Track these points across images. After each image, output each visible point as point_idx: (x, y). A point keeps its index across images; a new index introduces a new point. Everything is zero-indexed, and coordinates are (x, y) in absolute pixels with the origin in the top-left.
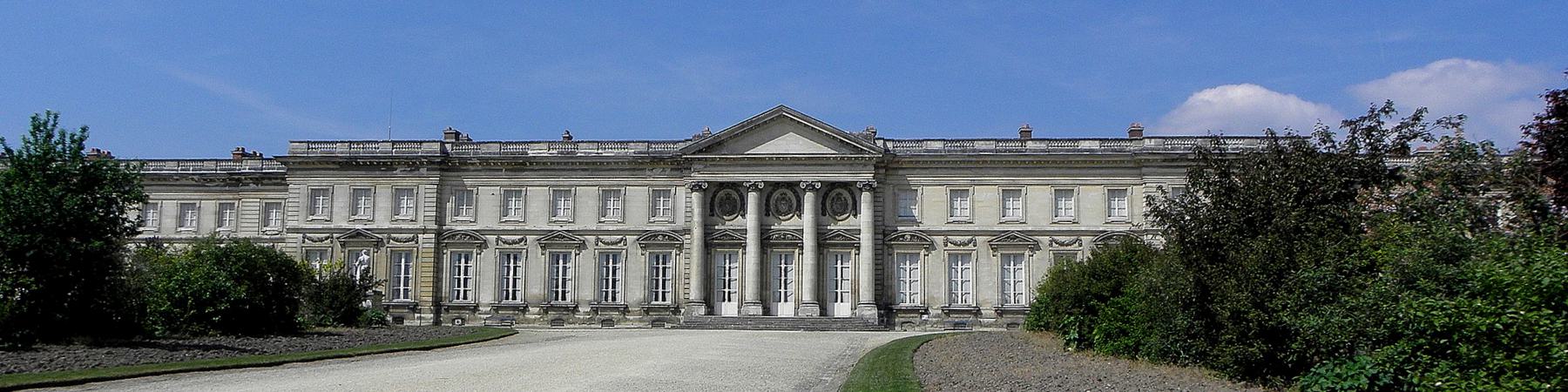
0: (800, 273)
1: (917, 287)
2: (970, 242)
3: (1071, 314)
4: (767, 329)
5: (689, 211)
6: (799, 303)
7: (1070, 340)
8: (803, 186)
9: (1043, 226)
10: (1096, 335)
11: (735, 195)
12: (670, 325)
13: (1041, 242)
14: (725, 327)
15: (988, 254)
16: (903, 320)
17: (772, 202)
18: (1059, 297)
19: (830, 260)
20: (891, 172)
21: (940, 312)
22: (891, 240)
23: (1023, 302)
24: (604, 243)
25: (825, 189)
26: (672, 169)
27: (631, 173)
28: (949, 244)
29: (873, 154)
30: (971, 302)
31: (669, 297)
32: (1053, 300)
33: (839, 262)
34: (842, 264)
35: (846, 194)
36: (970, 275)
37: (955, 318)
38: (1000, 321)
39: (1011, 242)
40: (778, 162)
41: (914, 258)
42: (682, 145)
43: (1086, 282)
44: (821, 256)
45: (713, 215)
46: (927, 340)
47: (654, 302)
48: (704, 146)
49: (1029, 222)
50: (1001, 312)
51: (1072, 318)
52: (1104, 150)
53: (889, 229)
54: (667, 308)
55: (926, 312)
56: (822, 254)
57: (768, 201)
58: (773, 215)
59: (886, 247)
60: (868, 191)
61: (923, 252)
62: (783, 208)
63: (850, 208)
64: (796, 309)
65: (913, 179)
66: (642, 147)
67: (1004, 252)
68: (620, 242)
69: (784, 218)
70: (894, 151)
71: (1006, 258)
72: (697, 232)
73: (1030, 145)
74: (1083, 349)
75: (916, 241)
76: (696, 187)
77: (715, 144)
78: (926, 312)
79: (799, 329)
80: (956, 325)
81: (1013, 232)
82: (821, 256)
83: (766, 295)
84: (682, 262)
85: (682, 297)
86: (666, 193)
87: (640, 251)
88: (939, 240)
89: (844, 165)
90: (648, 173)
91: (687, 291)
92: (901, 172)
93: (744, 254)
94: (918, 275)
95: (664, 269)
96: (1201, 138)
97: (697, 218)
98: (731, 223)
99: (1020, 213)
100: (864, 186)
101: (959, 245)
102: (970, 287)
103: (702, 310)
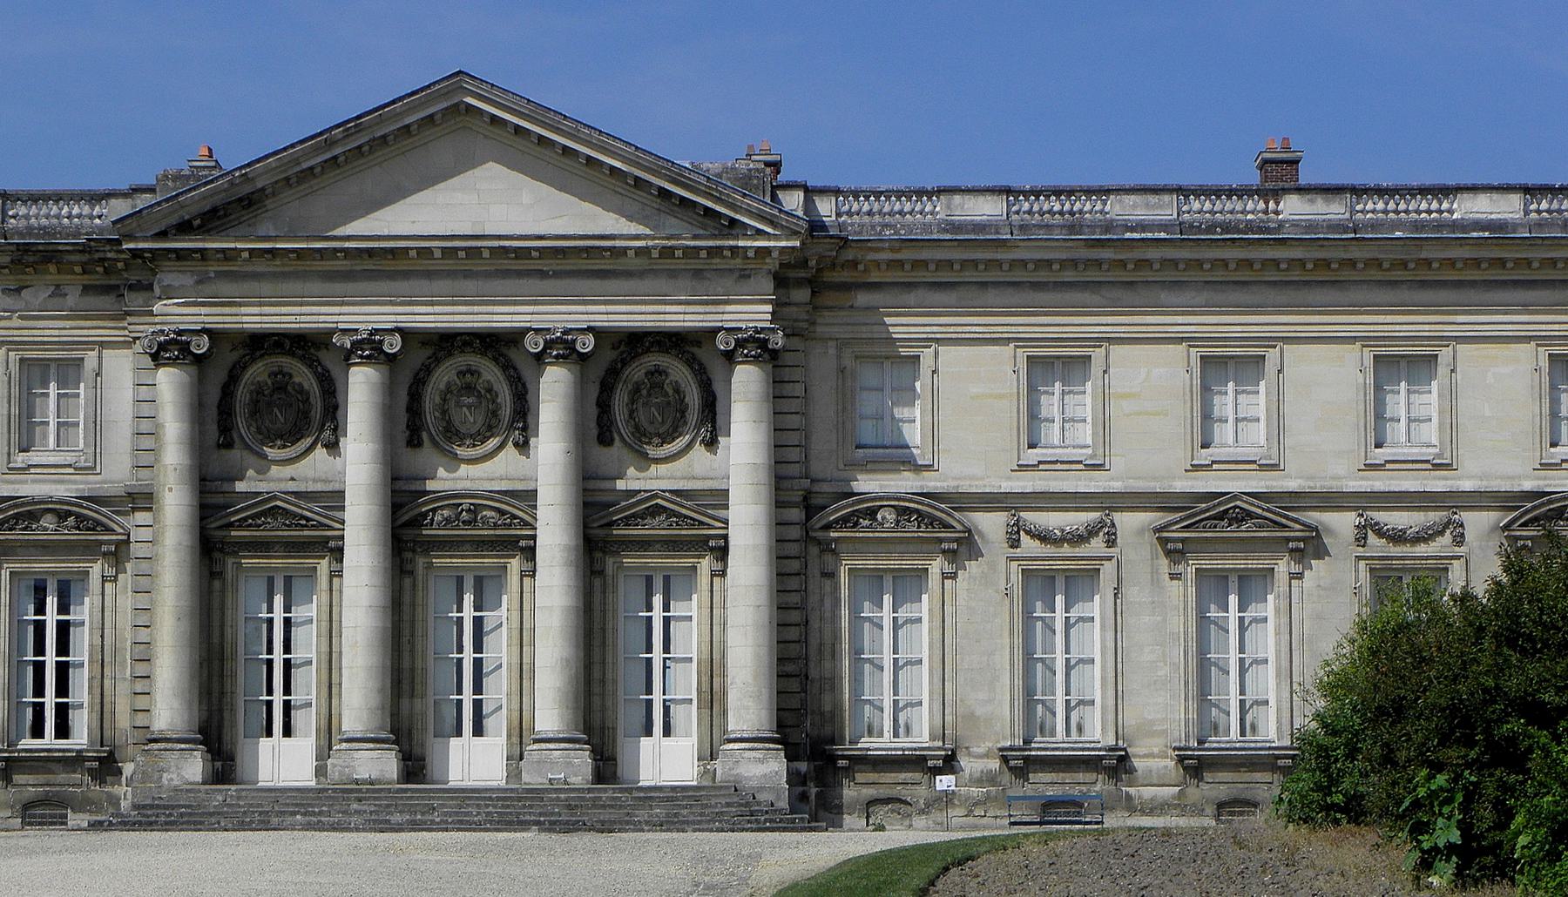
0: (524, 638)
1: (921, 684)
2: (1092, 532)
3: (1437, 767)
4: (415, 826)
5: (146, 433)
6: (521, 735)
7: (1435, 849)
8: (533, 344)
9: (1339, 478)
10: (1518, 834)
11: (303, 376)
12: (82, 819)
13: (1329, 531)
14: (275, 820)
15: (1154, 572)
16: (869, 792)
17: (431, 399)
18: (1397, 711)
19: (627, 593)
20: (829, 298)
21: (995, 764)
22: (828, 527)
23: (1272, 731)
25: (609, 355)
26: (86, 289)
28: (1024, 538)
29: (776, 237)
30: (1097, 734)
31: (81, 723)
32: (1375, 722)
33: (657, 600)
34: (666, 608)
35: (679, 373)
36: (1093, 641)
37: (1046, 784)
38: (1194, 793)
39: (1231, 532)
40: (449, 264)
41: (909, 583)
42: (120, 208)
43: (1486, 660)
44: (597, 582)
45: (228, 445)
46: (959, 857)
47: (28, 743)
48: (195, 209)
49: (1291, 463)
50: (1195, 766)
51: (1441, 780)
52: (1540, 225)
53: (825, 488)
54: (75, 761)
55: (949, 763)
56: (601, 573)
57: (415, 396)
58: (435, 444)
59: (814, 550)
60: (756, 360)
61: (936, 566)
62: (468, 416)
63: (693, 416)
64: (516, 758)
65: (901, 326)
67: (1206, 564)
70: (841, 227)
71: (1213, 585)
73: (1292, 207)
74: (1476, 882)
75: (912, 529)
76: (166, 351)
78: (949, 763)
79: (523, 825)
80: (1049, 805)
81: (1235, 497)
82: (597, 582)
83: (411, 716)
84: (126, 602)
85: (123, 721)
86: (68, 370)
88: (991, 524)
91: (141, 702)
92: (862, 298)
93: (336, 574)
94: (921, 641)
95: (63, 629)
97: (174, 455)
98: (288, 471)
99: (1258, 434)
100: (740, 344)
101: (1058, 542)
102: (1094, 682)
103: (192, 767)
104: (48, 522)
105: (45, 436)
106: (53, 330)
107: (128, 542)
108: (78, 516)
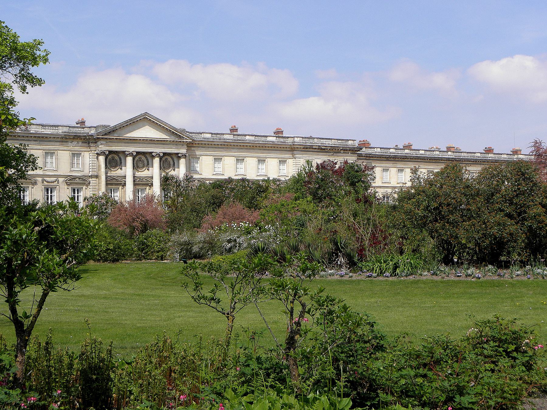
11: (117, 158)
24: (47, 182)
27: (61, 143)
29: (188, 140)
62: (141, 165)
65: (198, 153)
66: (66, 129)
68: (55, 181)
69: (114, 170)
72: (103, 178)
77: (113, 130)
87: (66, 187)
89: (173, 144)
90: (70, 144)
92: (193, 149)
95: (51, 196)
96: (316, 138)
98: (115, 172)
104: (77, 179)
105: (75, 165)
106: (77, 148)
107: (90, 183)
108: (82, 179)
